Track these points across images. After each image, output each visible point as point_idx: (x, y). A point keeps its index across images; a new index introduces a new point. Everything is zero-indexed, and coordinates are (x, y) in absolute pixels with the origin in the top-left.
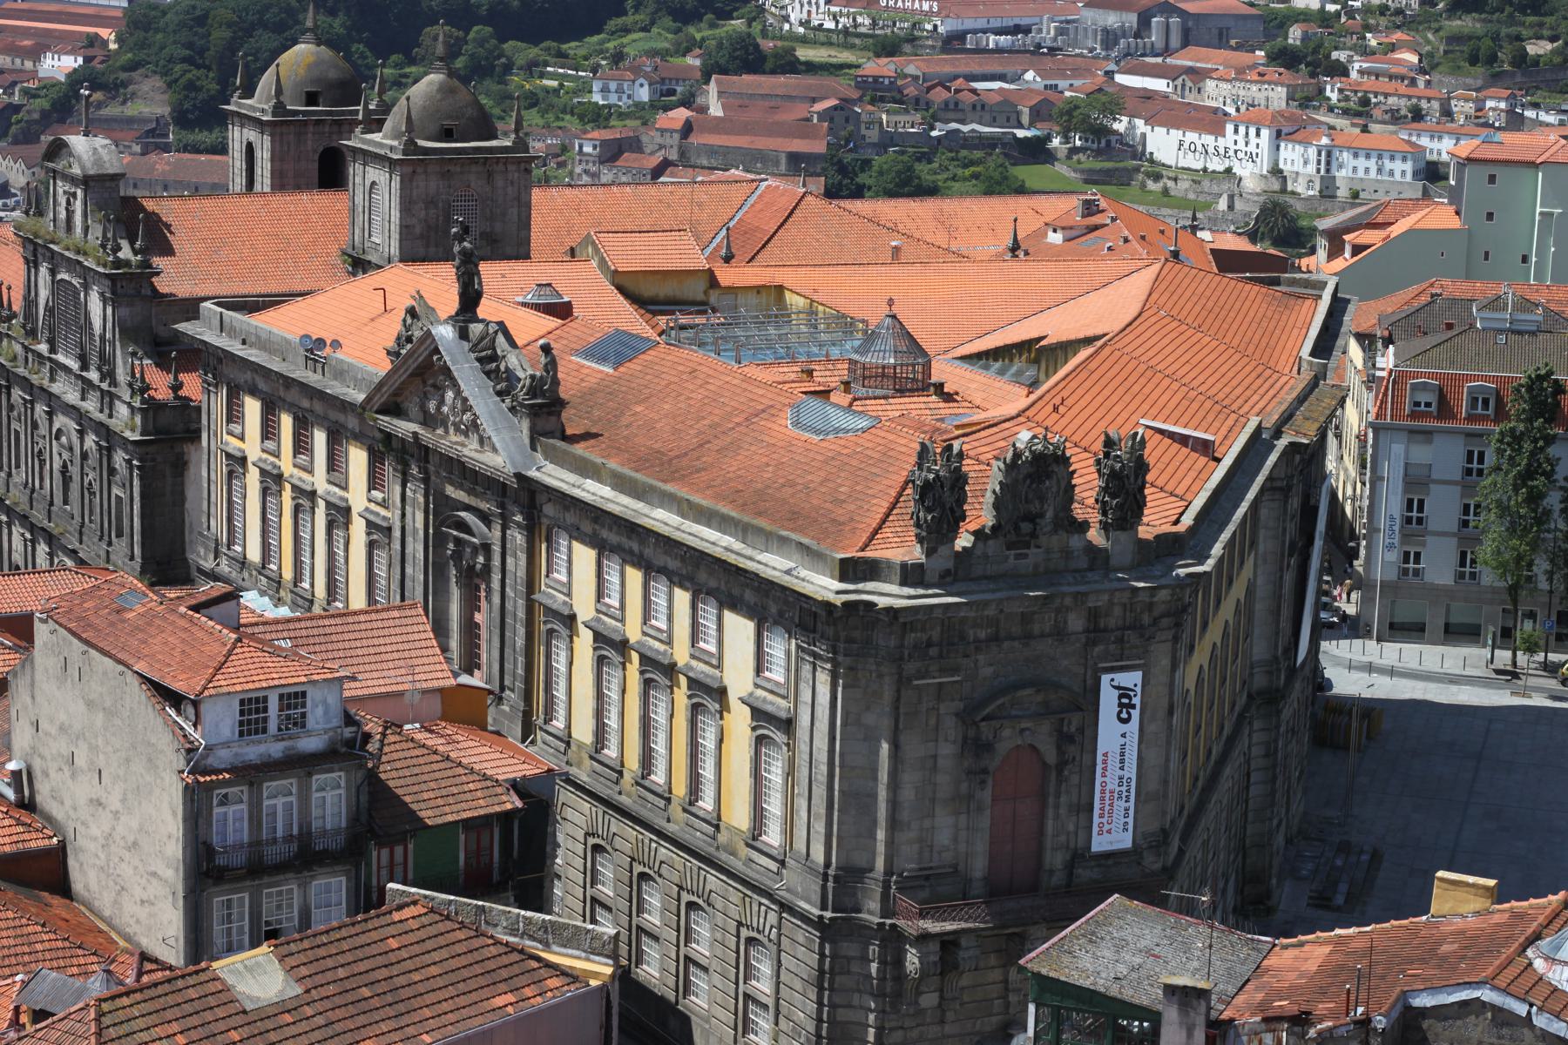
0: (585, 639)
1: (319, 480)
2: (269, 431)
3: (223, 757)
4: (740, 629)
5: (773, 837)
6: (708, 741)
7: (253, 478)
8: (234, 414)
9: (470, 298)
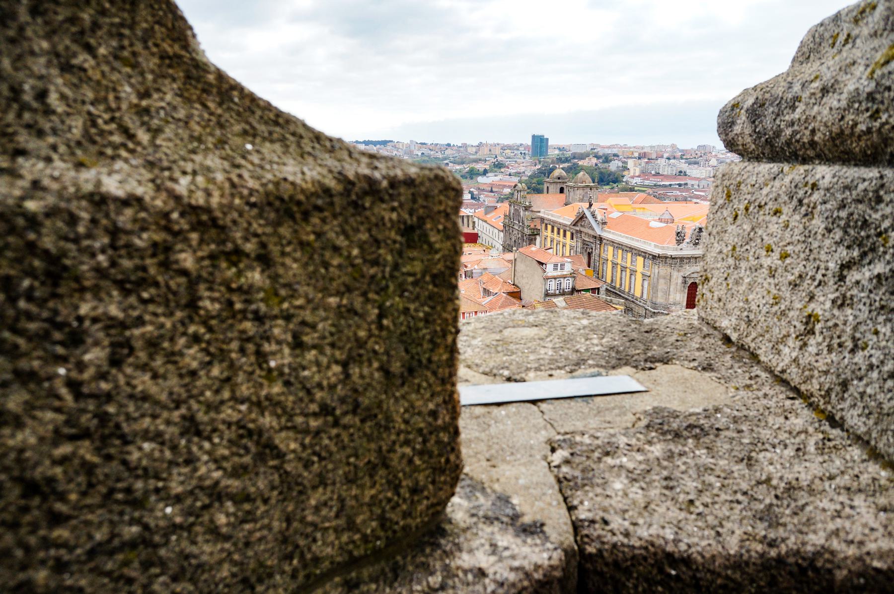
0: (610, 265)
1: (561, 239)
2: (553, 231)
3: (550, 274)
4: (640, 260)
5: (645, 297)
6: (633, 281)
7: (549, 240)
8: (546, 229)
9: (591, 205)
